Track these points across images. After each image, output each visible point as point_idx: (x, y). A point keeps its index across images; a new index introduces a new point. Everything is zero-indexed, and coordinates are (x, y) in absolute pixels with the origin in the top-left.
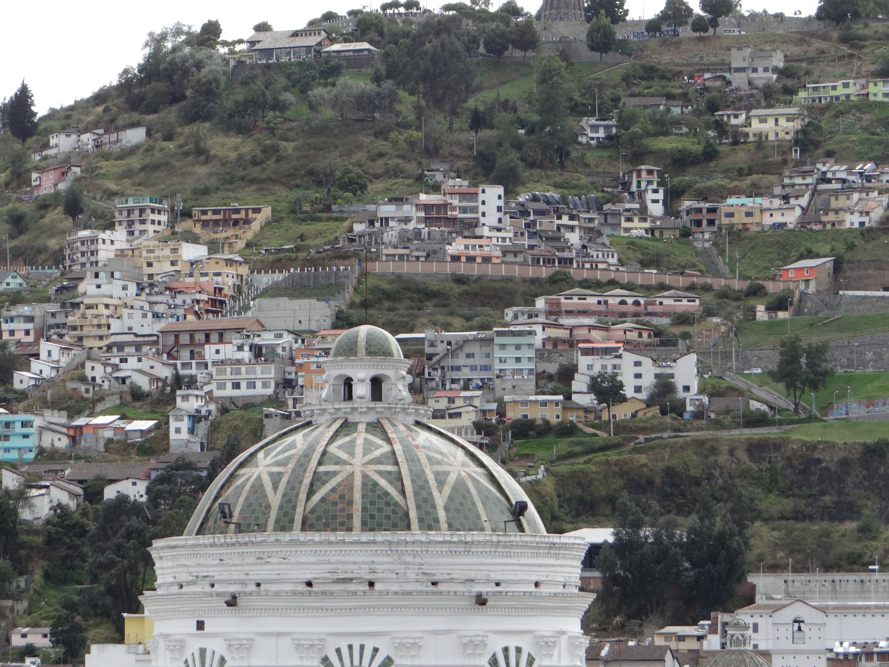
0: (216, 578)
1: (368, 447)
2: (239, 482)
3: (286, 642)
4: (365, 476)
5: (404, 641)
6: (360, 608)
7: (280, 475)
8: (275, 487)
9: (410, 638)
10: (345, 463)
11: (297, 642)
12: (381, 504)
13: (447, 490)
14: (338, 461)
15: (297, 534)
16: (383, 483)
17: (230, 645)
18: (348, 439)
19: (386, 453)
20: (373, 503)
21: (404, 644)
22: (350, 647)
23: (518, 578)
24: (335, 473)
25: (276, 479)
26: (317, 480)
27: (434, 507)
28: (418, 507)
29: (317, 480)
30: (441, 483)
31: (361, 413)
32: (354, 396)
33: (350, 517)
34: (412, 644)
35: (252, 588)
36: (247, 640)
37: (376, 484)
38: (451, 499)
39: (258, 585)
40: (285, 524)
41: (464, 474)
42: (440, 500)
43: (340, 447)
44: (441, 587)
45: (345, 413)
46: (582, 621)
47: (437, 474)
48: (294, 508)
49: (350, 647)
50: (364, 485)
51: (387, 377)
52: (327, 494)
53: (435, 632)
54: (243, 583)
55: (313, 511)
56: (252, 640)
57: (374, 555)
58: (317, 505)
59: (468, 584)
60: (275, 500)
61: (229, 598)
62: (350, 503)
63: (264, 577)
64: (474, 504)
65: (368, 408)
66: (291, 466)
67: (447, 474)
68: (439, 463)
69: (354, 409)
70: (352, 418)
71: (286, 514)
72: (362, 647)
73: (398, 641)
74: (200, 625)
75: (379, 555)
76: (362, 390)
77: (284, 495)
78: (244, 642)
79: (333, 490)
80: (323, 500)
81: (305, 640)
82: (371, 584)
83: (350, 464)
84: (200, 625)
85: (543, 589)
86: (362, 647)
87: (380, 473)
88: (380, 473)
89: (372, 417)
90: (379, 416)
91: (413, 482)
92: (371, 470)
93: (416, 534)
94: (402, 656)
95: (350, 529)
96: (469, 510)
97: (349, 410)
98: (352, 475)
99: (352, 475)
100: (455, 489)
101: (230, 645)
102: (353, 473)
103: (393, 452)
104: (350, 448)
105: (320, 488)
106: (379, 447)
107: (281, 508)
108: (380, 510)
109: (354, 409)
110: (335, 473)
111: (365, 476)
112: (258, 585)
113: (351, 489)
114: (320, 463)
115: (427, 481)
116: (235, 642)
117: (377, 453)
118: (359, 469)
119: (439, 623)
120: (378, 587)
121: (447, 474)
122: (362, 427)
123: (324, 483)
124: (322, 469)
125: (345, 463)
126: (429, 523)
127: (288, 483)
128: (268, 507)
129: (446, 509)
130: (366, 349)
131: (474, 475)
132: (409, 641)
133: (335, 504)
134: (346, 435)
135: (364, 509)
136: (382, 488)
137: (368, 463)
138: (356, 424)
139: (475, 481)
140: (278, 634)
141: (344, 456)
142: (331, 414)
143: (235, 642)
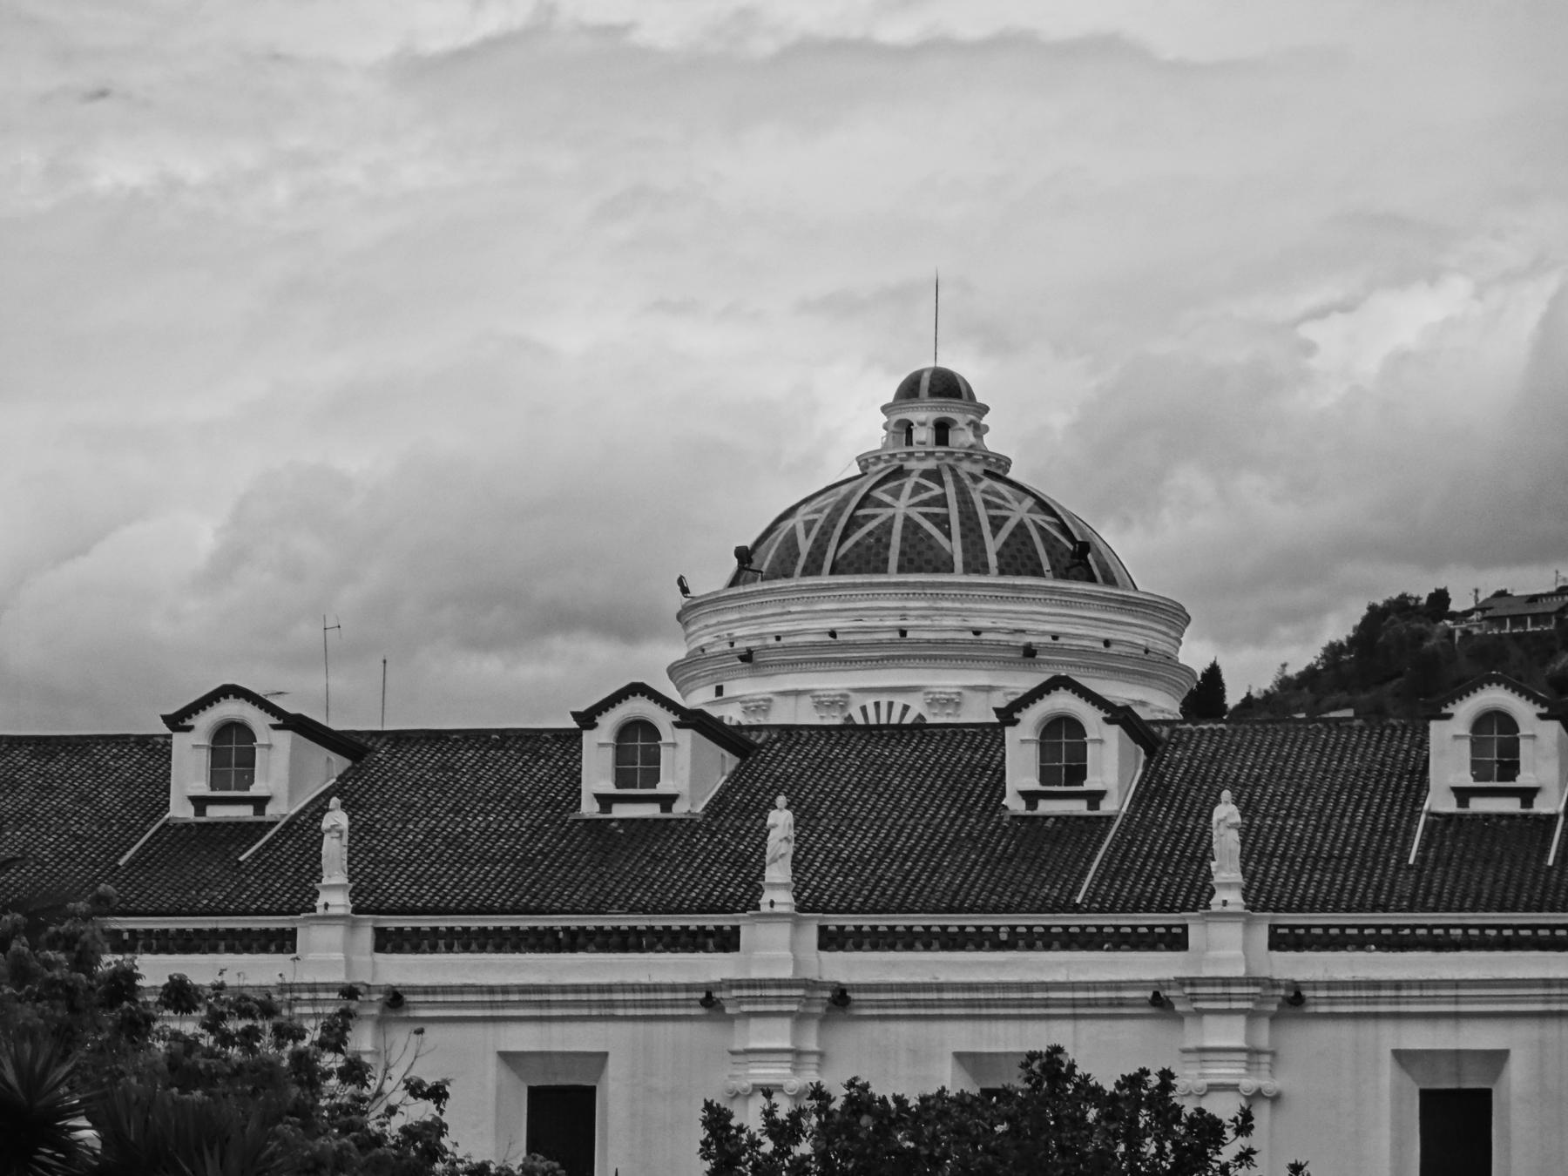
0: (736, 635)
1: (918, 489)
2: (772, 536)
3: (807, 701)
4: (907, 519)
5: (937, 696)
6: (888, 658)
7: (815, 521)
8: (808, 533)
9: (945, 693)
10: (888, 505)
11: (817, 700)
12: (922, 547)
13: (1004, 534)
14: (881, 504)
15: (825, 579)
16: (927, 525)
17: (746, 708)
18: (896, 483)
19: (937, 496)
20: (913, 546)
21: (938, 700)
22: (877, 705)
23: (1080, 632)
24: (874, 517)
25: (809, 526)
26: (854, 523)
27: (984, 551)
28: (965, 550)
29: (854, 523)
30: (997, 524)
31: (920, 459)
32: (914, 442)
33: (886, 561)
34: (948, 700)
35: (772, 641)
36: (764, 700)
37: (918, 526)
38: (1006, 544)
39: (778, 638)
40: (813, 568)
41: (1027, 521)
42: (992, 546)
43: (884, 491)
44: (984, 636)
45: (901, 459)
46: (1183, 703)
47: (992, 519)
48: (824, 553)
49: (877, 705)
50: (905, 527)
51: (954, 422)
52: (864, 538)
53: (974, 688)
54: (760, 636)
55: (845, 556)
56: (770, 700)
57: (906, 599)
58: (850, 550)
59: (1018, 635)
60: (805, 546)
61: (744, 652)
62: (887, 546)
63: (784, 629)
64: (1035, 552)
65: (926, 452)
66: (827, 511)
67: (1006, 518)
68: (999, 507)
69: (910, 454)
70: (908, 465)
71: (814, 561)
72: (891, 705)
73: (931, 696)
74: (719, 691)
75: (911, 599)
76: (923, 435)
77: (816, 540)
78: (761, 703)
79: (870, 534)
80: (857, 544)
81: (824, 696)
82: (903, 633)
83: (892, 506)
84: (719, 691)
85: (1113, 649)
86: (891, 705)
87: (925, 515)
88: (925, 515)
89: (930, 464)
90: (939, 462)
91: (962, 524)
92: (915, 514)
93: (958, 577)
94: (935, 714)
95: (884, 571)
96: (1029, 558)
97: (904, 456)
98: (893, 518)
99: (893, 518)
100: (1013, 534)
101: (746, 708)
102: (894, 516)
103: (944, 495)
104: (896, 494)
105: (854, 532)
106: (931, 489)
107: (810, 554)
108: (920, 553)
109: (910, 454)
110: (874, 517)
111: (907, 519)
112: (778, 638)
113: (889, 532)
114: (859, 506)
115: (979, 524)
116: (751, 704)
117: (925, 496)
118: (902, 511)
119: (981, 678)
120: (910, 635)
121: (1006, 518)
122: (916, 474)
123: (862, 526)
124: (861, 512)
125: (888, 505)
126: (976, 564)
127: (822, 527)
128: (798, 554)
129: (999, 554)
130: (930, 390)
131: (1047, 527)
132: (943, 696)
133: (869, 548)
134: (895, 480)
135: (902, 553)
136: (925, 530)
137: (914, 505)
138: (912, 471)
139: (1040, 529)
140: (798, 693)
141: (887, 499)
142: (886, 461)
143: (751, 704)
